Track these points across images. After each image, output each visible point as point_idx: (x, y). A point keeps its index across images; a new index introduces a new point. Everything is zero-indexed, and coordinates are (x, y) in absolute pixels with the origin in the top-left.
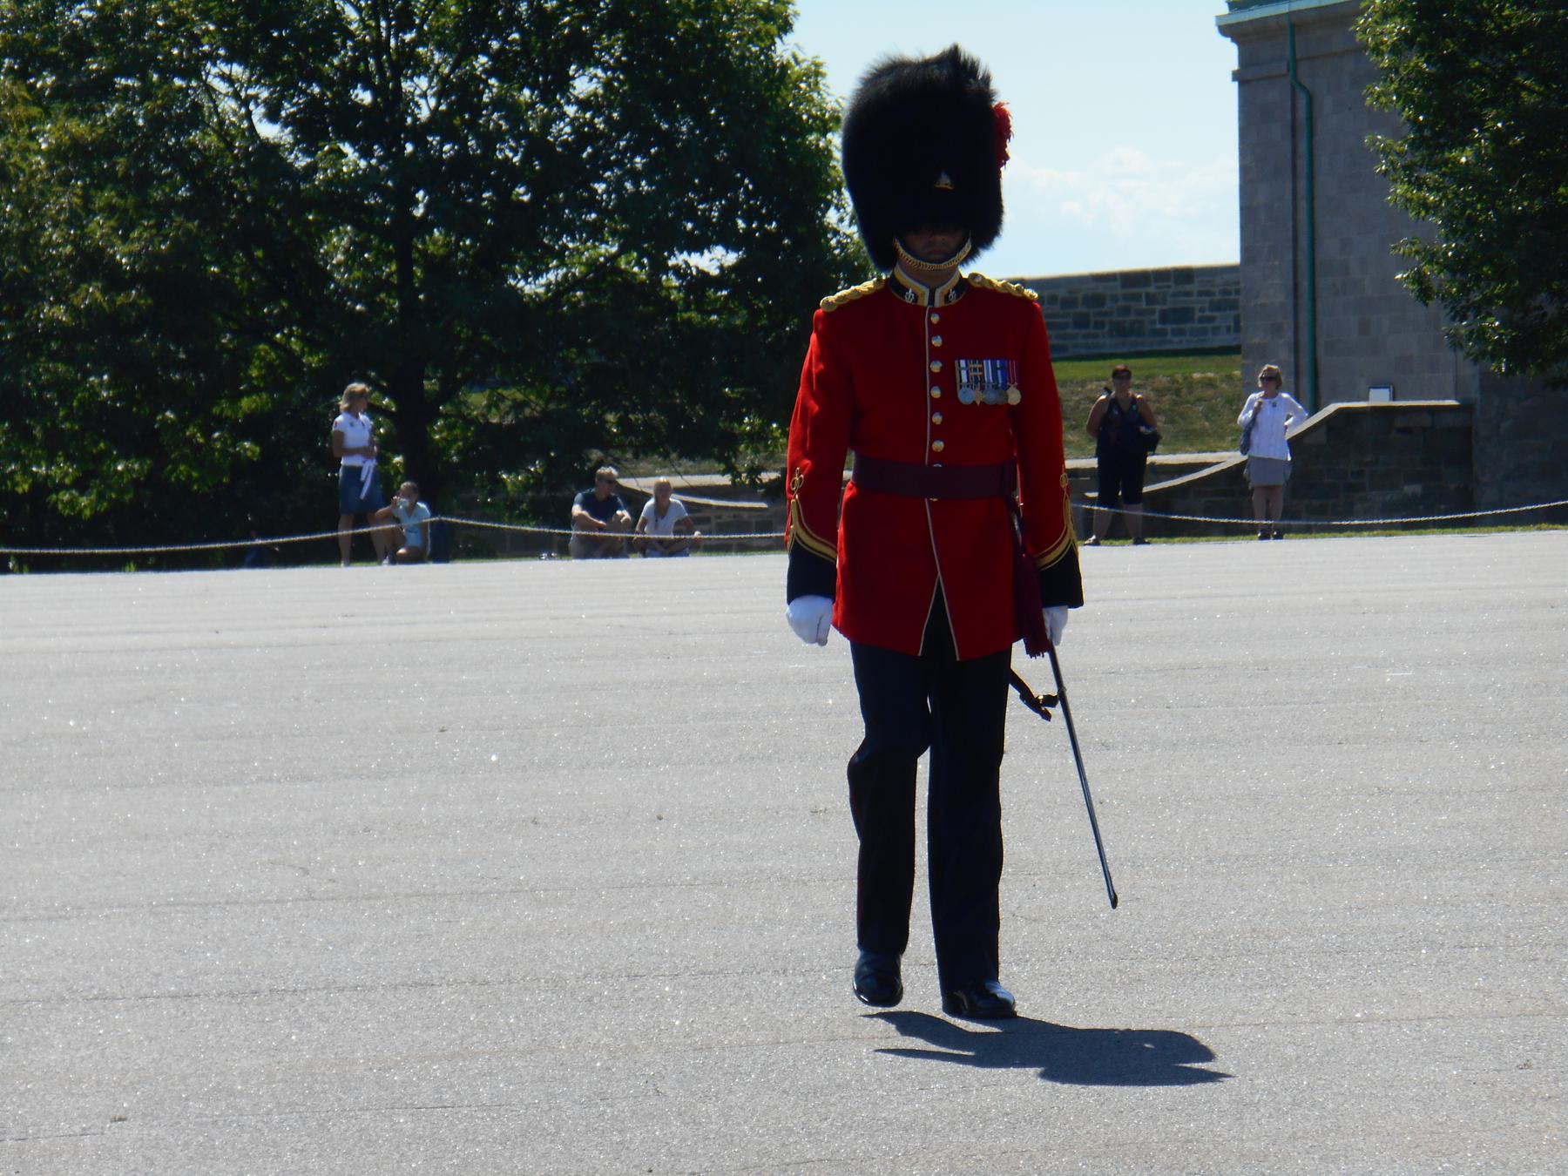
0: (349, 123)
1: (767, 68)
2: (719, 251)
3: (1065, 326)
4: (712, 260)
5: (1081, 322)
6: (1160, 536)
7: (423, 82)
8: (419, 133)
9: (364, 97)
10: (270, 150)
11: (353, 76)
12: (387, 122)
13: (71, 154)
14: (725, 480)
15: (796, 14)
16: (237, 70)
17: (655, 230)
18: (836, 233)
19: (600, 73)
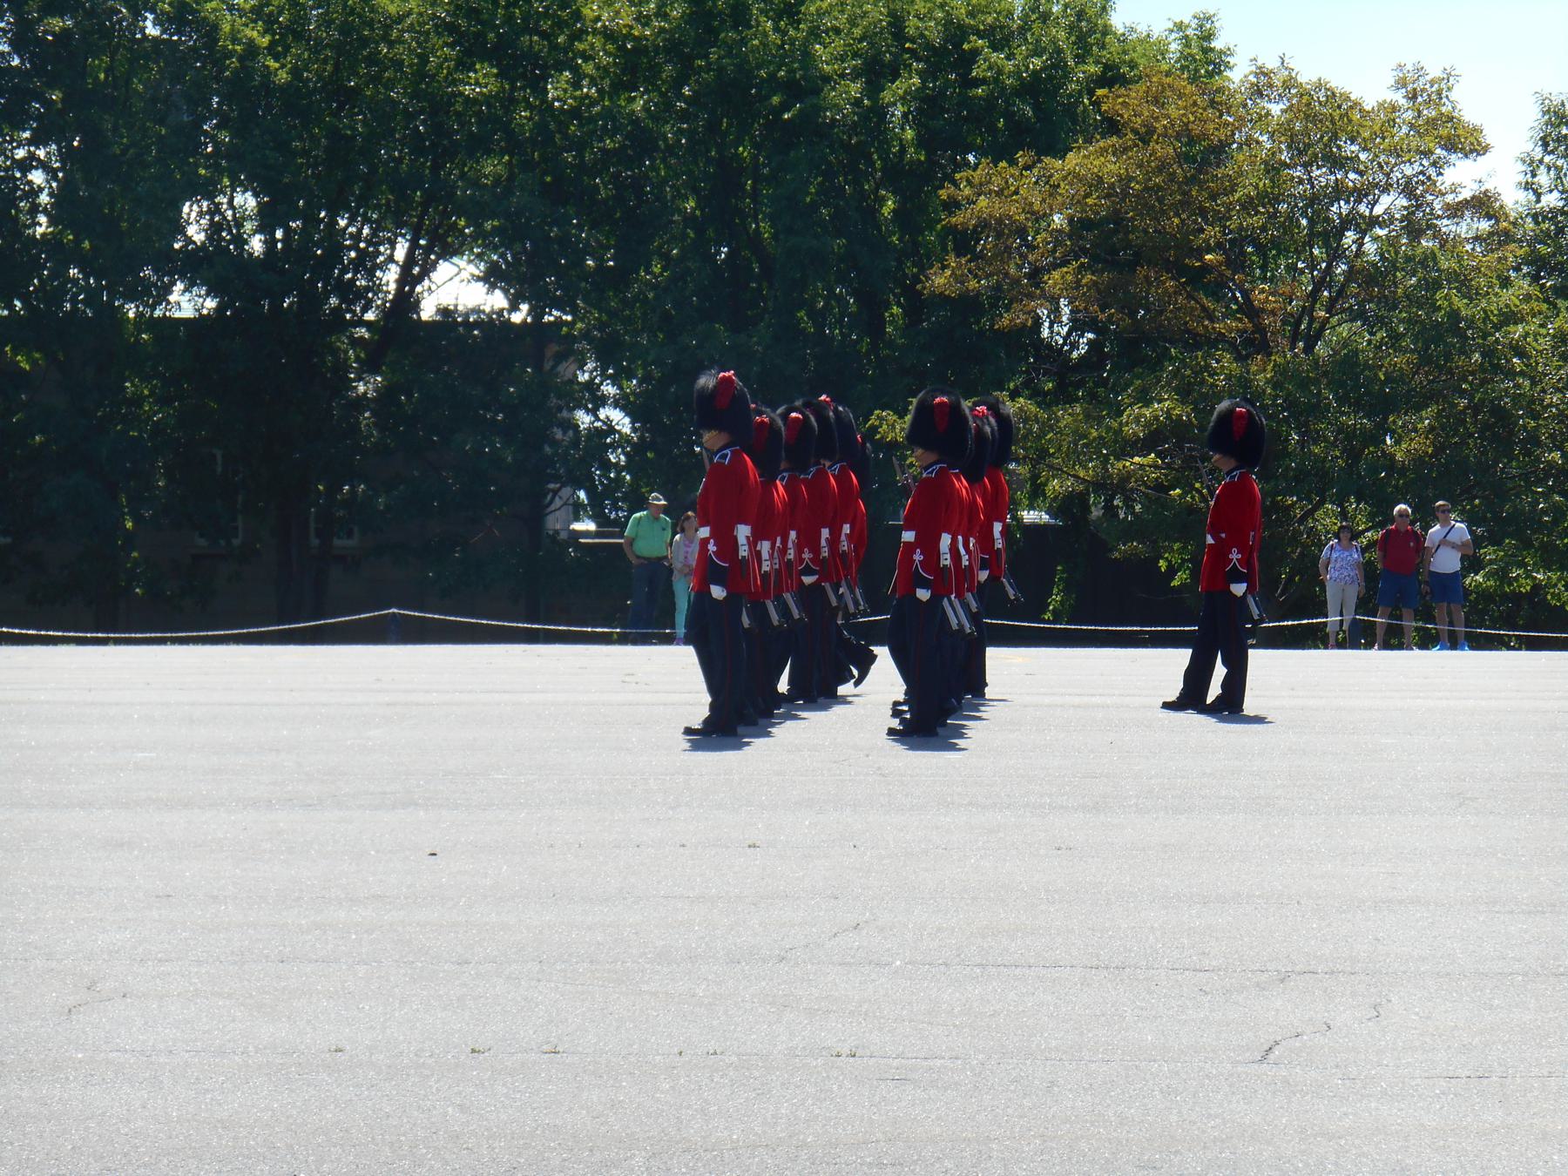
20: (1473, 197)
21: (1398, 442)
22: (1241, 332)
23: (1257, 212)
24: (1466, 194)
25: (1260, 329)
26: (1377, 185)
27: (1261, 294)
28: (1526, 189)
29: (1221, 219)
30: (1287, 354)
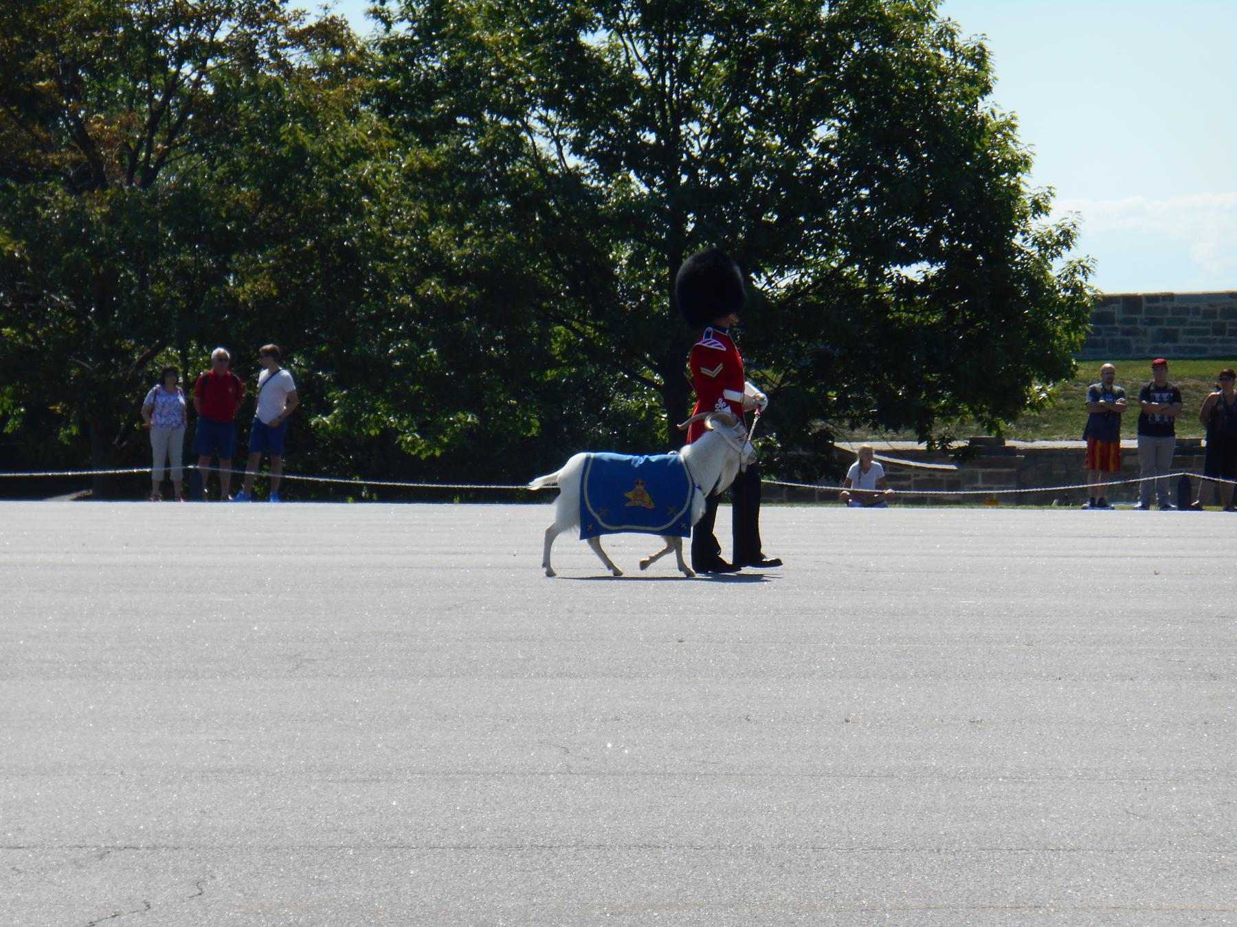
0: (639, 159)
1: (970, 121)
2: (925, 265)
3: (1206, 332)
4: (915, 272)
5: (1219, 330)
6: (1210, 504)
7: (695, 127)
8: (691, 166)
9: (651, 138)
10: (573, 177)
11: (642, 120)
12: (666, 158)
13: (420, 176)
14: (923, 446)
15: (995, 79)
16: (552, 115)
17: (877, 248)
18: (1021, 252)
19: (837, 123)
20: (319, 25)
21: (241, 283)
22: (75, 164)
23: (92, 37)
24: (311, 21)
25: (97, 162)
26: (218, 11)
27: (97, 124)
28: (376, 17)
29: (52, 43)
30: (124, 187)
